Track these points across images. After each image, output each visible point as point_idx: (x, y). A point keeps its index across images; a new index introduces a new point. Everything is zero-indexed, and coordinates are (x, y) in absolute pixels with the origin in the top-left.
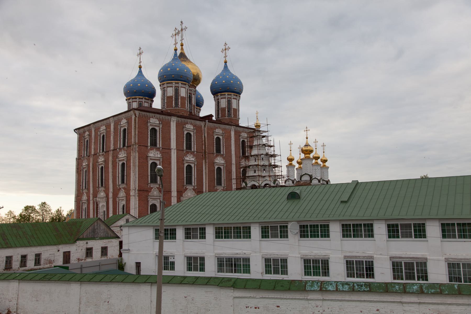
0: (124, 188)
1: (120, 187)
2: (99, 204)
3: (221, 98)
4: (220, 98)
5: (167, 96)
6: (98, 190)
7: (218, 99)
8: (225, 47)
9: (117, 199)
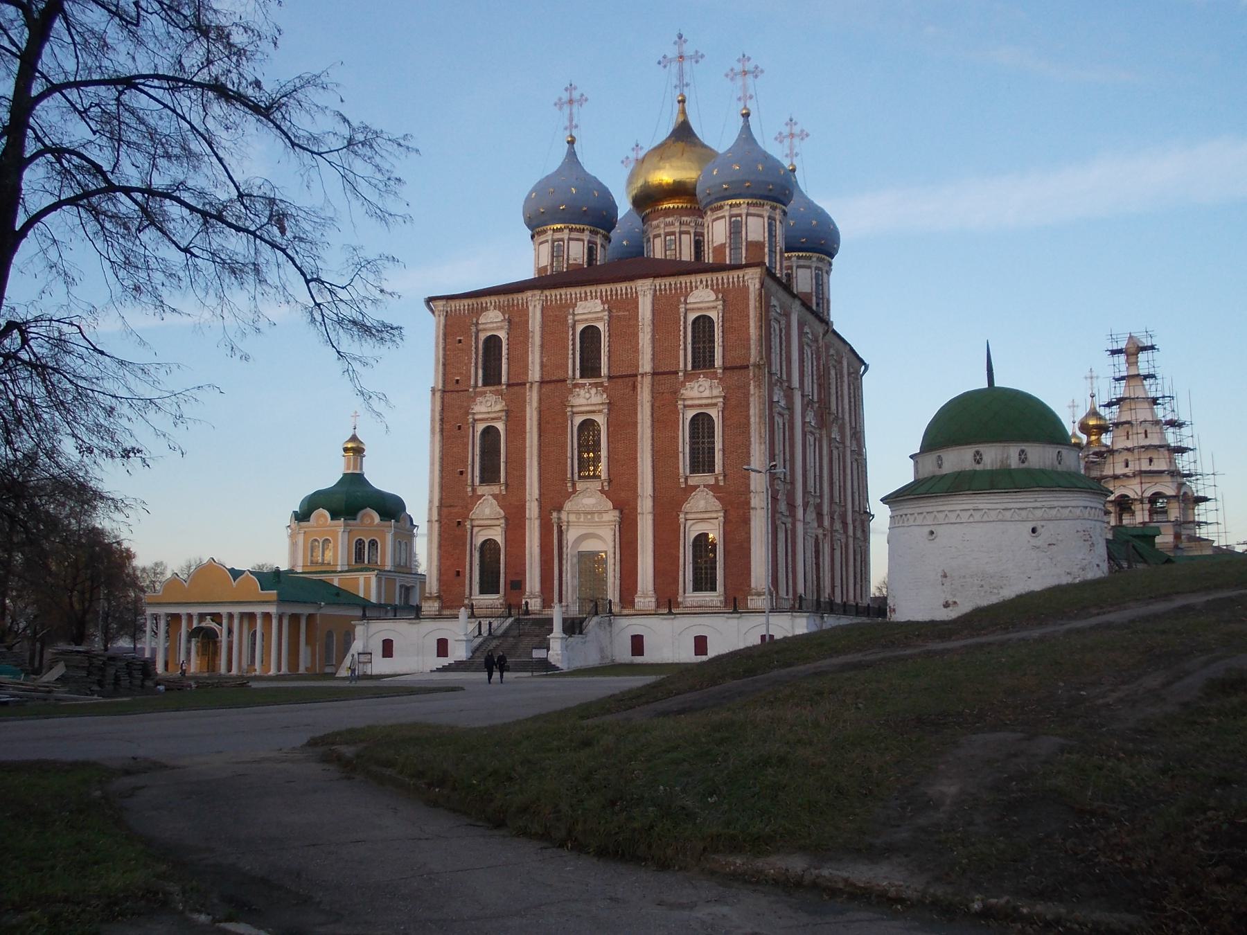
0: (714, 488)
1: (690, 482)
2: (567, 530)
3: (798, 267)
4: (795, 265)
5: (746, 239)
6: (570, 490)
7: (790, 268)
8: (791, 128)
9: (682, 516)
